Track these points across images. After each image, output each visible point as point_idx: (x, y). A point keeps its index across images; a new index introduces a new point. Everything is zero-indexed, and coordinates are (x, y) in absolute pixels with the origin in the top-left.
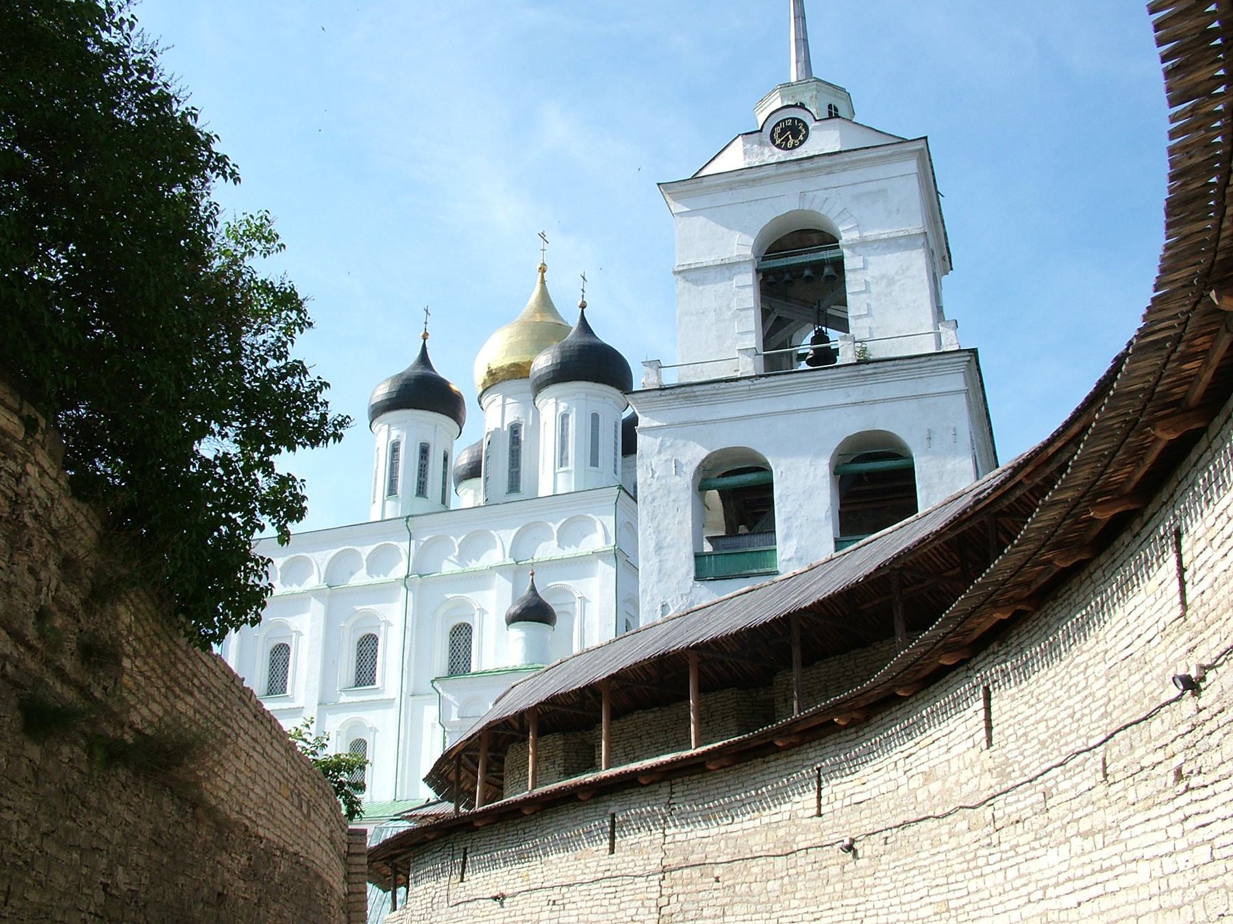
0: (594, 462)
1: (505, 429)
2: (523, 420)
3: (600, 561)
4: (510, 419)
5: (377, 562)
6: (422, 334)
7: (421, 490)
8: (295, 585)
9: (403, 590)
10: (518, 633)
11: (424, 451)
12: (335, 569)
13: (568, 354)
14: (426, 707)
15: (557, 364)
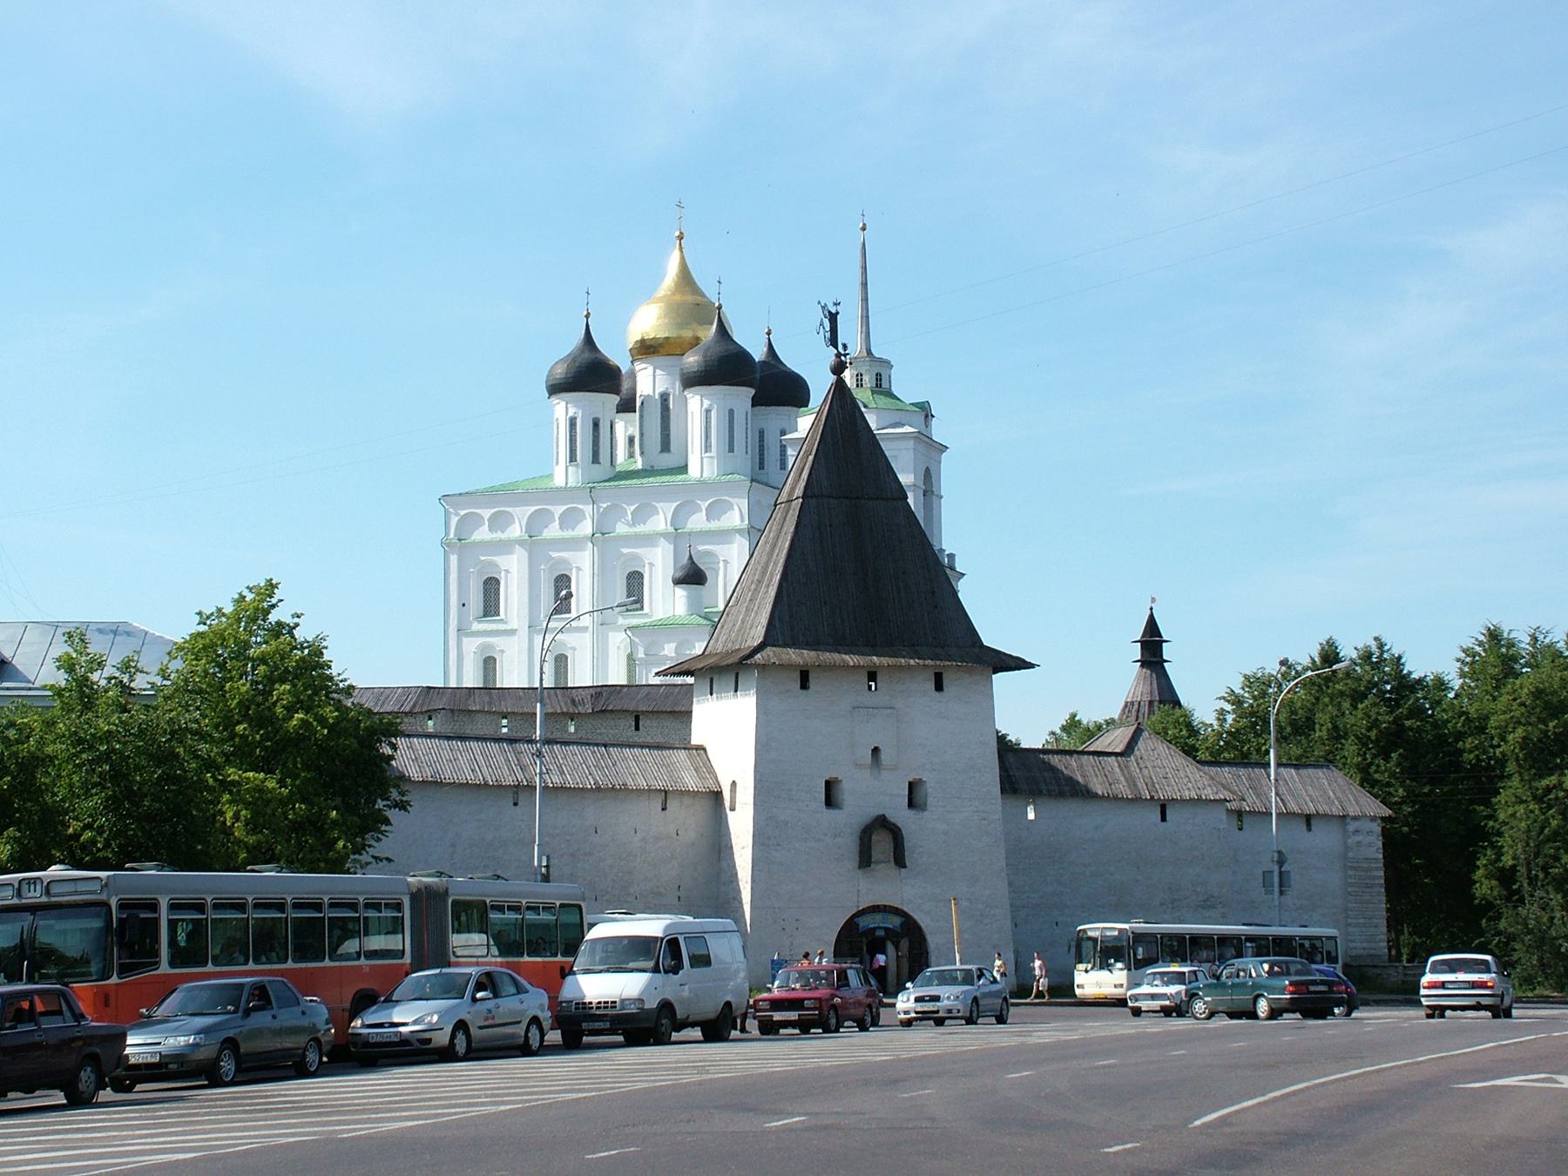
0: (731, 450)
1: (657, 397)
2: (671, 390)
3: (737, 535)
4: (660, 389)
5: (569, 519)
6: (585, 313)
7: (596, 459)
8: (499, 532)
9: (590, 545)
10: (681, 592)
11: (596, 424)
12: (535, 524)
13: (710, 363)
14: (610, 634)
15: (702, 371)
